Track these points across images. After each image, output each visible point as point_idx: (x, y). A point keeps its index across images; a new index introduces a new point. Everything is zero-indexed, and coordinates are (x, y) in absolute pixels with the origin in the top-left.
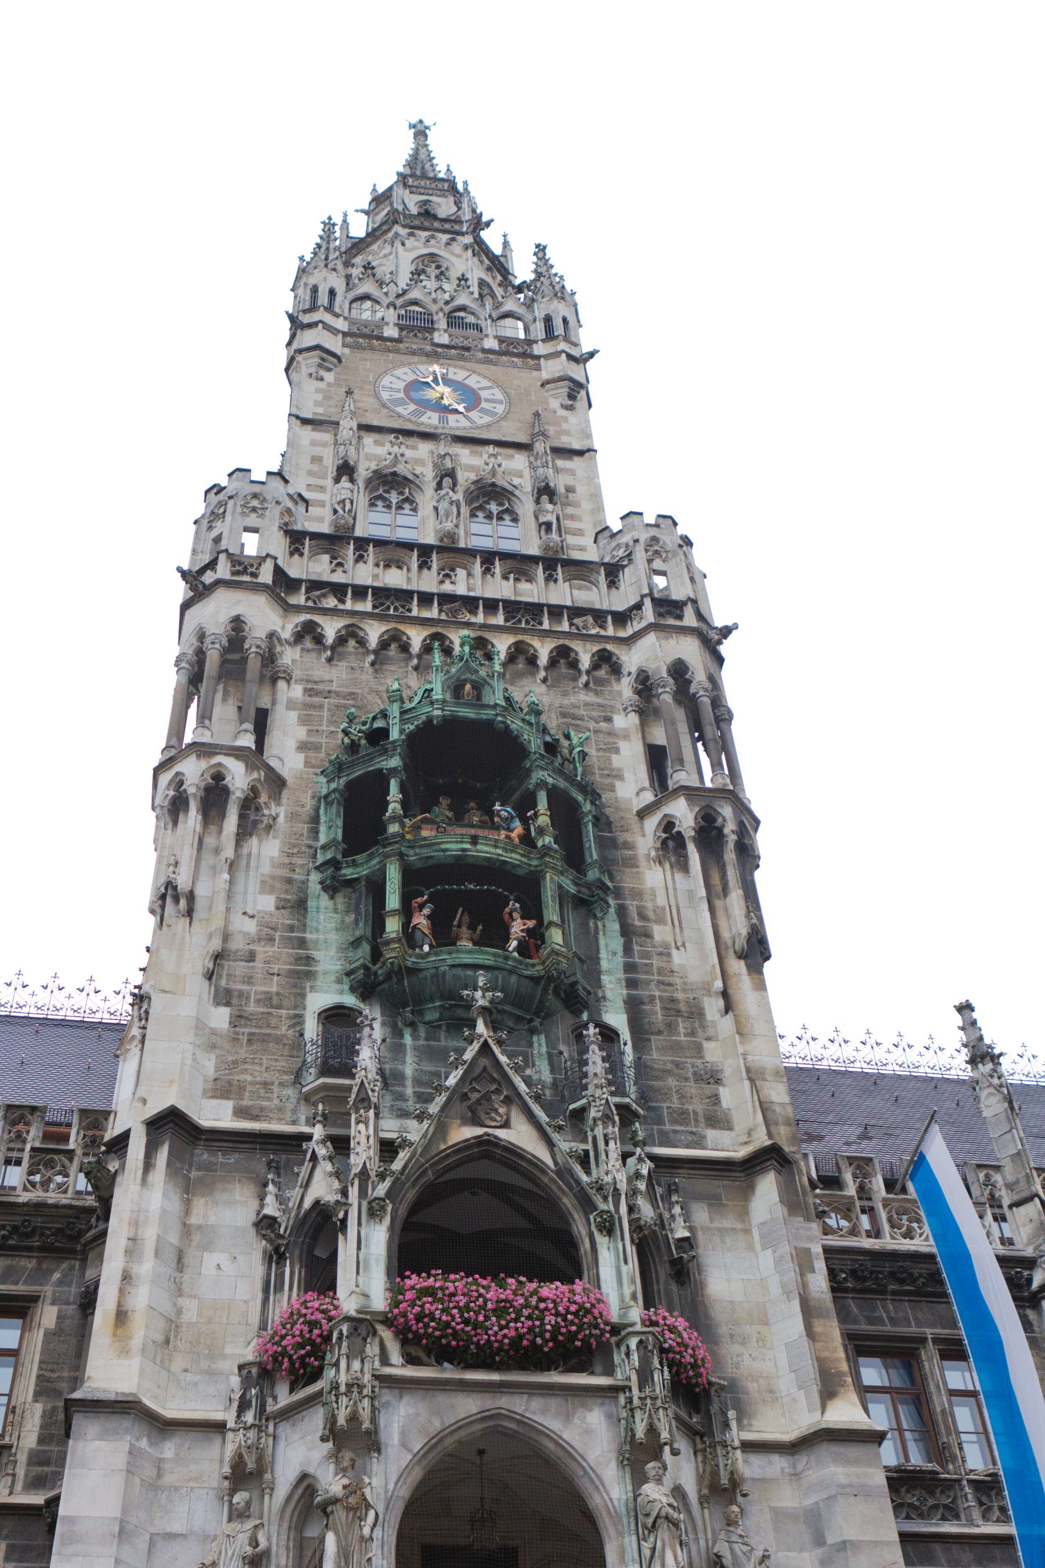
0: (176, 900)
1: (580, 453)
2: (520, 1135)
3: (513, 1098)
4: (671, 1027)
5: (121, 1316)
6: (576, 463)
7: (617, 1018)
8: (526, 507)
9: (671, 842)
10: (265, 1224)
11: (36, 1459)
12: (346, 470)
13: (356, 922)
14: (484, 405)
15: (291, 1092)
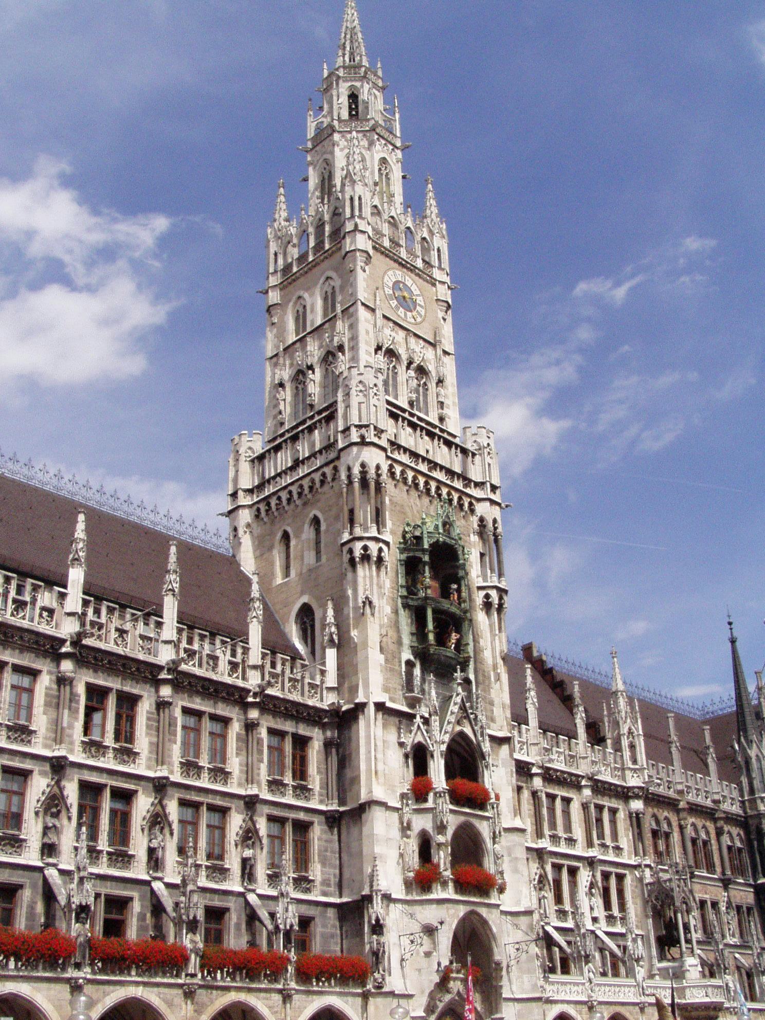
0: (370, 607)
1: (449, 354)
2: (468, 730)
3: (467, 717)
4: (484, 681)
5: (376, 772)
6: (446, 359)
7: (472, 677)
8: (432, 385)
9: (487, 606)
10: (401, 745)
11: (321, 795)
12: (379, 348)
13: (412, 623)
14: (418, 308)
15: (401, 693)
